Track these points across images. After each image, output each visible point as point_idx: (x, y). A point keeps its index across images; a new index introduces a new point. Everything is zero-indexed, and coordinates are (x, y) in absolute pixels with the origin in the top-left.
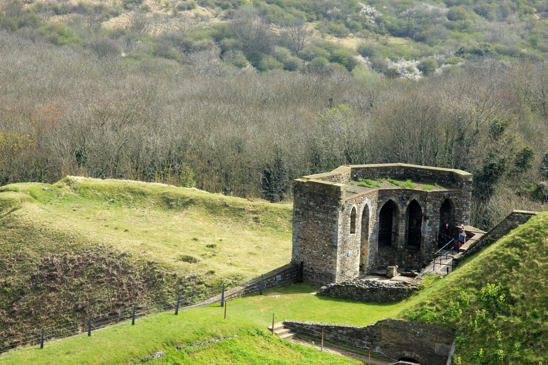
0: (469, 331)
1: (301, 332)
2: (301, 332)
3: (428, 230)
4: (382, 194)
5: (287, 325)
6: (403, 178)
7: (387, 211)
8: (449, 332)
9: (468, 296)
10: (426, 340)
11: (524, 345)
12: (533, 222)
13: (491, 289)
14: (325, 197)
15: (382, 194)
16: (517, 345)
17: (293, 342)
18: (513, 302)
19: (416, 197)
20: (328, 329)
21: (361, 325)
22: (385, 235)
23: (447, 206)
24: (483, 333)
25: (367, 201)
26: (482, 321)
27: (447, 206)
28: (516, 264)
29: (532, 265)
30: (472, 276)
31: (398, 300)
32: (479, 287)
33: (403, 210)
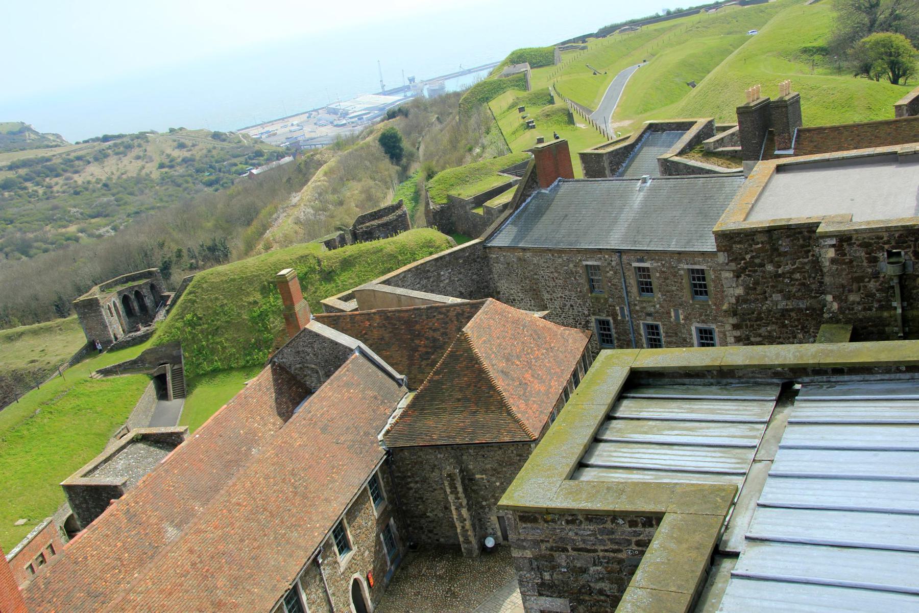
0: (186, 339)
1: (106, 372)
2: (106, 372)
3: (149, 302)
4: (119, 293)
5: (98, 372)
6: (126, 282)
7: (125, 300)
8: (177, 344)
9: (179, 324)
10: (168, 352)
11: (213, 336)
12: (195, 279)
13: (189, 317)
14: (91, 305)
15: (119, 293)
16: (210, 337)
18: (200, 319)
19: (136, 289)
20: (119, 366)
21: (134, 357)
22: (129, 312)
23: (153, 287)
24: (193, 338)
25: (113, 299)
26: (190, 333)
27: (153, 287)
28: (195, 301)
29: (202, 299)
30: (178, 314)
31: (148, 339)
32: (182, 318)
33: (133, 297)
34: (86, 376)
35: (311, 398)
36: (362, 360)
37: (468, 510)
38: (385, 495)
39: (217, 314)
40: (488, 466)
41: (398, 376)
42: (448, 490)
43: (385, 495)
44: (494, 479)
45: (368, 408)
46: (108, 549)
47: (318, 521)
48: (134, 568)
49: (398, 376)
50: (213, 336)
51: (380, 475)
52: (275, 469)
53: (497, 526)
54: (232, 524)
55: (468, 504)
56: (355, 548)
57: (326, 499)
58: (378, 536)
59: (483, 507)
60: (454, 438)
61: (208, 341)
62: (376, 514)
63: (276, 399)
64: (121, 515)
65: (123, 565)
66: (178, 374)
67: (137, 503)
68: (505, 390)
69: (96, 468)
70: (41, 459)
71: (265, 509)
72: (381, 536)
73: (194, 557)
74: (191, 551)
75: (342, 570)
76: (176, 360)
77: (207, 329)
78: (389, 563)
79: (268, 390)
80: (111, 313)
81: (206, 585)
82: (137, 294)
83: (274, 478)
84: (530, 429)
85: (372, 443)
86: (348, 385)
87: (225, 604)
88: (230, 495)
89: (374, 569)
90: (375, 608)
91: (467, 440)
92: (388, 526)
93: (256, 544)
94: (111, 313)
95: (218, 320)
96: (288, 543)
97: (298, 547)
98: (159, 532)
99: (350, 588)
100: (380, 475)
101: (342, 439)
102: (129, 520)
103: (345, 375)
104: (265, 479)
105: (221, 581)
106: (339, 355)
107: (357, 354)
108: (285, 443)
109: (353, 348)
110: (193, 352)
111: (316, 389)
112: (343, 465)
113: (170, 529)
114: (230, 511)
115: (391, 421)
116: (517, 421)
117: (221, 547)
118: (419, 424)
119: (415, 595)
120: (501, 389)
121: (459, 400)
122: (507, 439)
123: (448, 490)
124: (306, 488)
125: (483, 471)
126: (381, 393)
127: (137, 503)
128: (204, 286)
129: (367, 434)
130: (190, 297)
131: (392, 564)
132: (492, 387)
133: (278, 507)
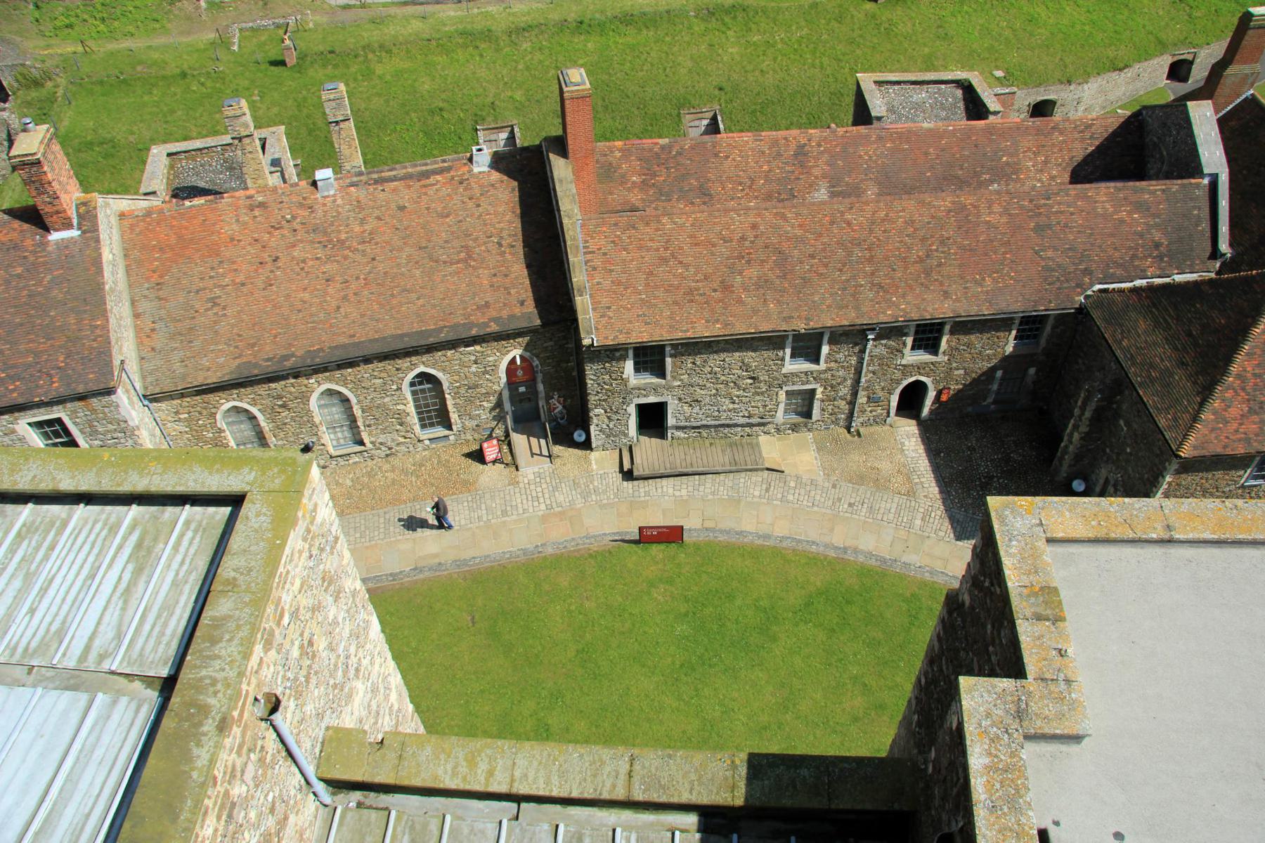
35: (1138, 183)
36: (1202, 195)
37: (1081, 438)
38: (1043, 342)
40: (1135, 426)
41: (1224, 246)
42: (1079, 403)
43: (1043, 342)
44: (1129, 441)
45: (1131, 248)
46: (752, 164)
47: (908, 303)
48: (756, 197)
49: (1224, 246)
51: (1051, 322)
52: (929, 223)
53: (1102, 481)
54: (820, 235)
55: (1087, 434)
56: (942, 358)
57: (946, 292)
58: (993, 370)
59: (1104, 451)
60: (1133, 364)
62: (1009, 349)
63: (1090, 155)
64: (793, 146)
65: (750, 187)
67: (819, 145)
68: (1238, 376)
69: (898, 83)
70: (1087, 28)
71: (869, 249)
72: (999, 374)
73: (750, 235)
74: (754, 226)
75: (904, 362)
78: (990, 400)
79: (1091, 138)
81: (734, 264)
83: (916, 230)
84: (1192, 439)
85: (1078, 286)
86: (1139, 206)
87: (733, 292)
88: (851, 208)
89: (960, 391)
90: (930, 419)
91: (1137, 380)
92: (1026, 370)
93: (822, 270)
96: (853, 296)
97: (857, 308)
98: (811, 186)
99: (905, 383)
100: (1051, 322)
101: (1050, 254)
102: (796, 155)
103: (1153, 193)
104: (906, 222)
105: (753, 272)
106: (1188, 165)
107: (1206, 181)
108: (975, 207)
109: (1206, 171)
111: (1150, 179)
112: (1012, 278)
113: (823, 191)
114: (832, 223)
115: (1139, 283)
116: (1195, 419)
117: (785, 245)
118: (1133, 315)
119: (969, 448)
120: (1234, 369)
121: (1190, 334)
122: (1162, 422)
123: (1079, 403)
124: (940, 265)
125: (1128, 424)
126: (1174, 247)
127: (819, 145)
129: (1087, 272)
131: (995, 402)
132: (1229, 360)
133: (886, 258)
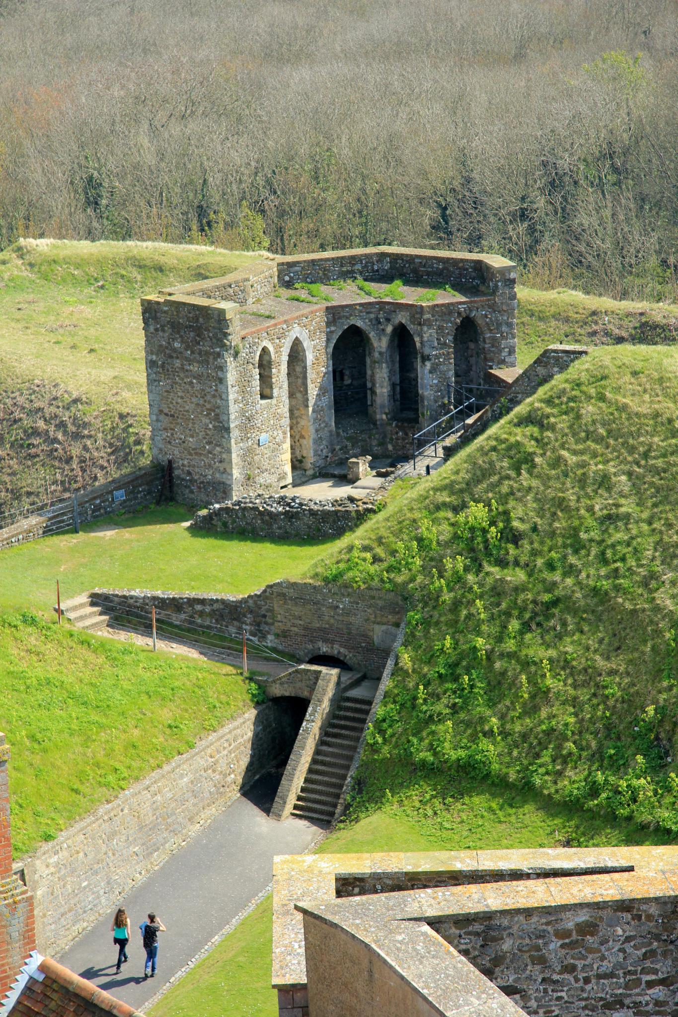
0: (431, 599)
1: (123, 612)
2: (123, 612)
4: (334, 314)
5: (96, 600)
7: (349, 347)
8: (398, 602)
9: (437, 531)
10: (357, 620)
11: (526, 627)
13: (477, 513)
14: (198, 331)
15: (334, 314)
17: (105, 633)
18: (515, 538)
19: (402, 318)
20: (175, 604)
21: (234, 594)
24: (456, 605)
25: (296, 332)
29: (557, 462)
30: (449, 487)
32: (456, 510)
33: (380, 344)
34: (40, 599)
39: (578, 547)
50: (526, 627)
61: (500, 639)
66: (348, 717)
76: (362, 666)
77: (517, 590)
80: (266, 379)
82: (402, 339)
94: (266, 379)
95: (570, 571)
110: (431, 660)
128: (589, 410)
130: (520, 435)
